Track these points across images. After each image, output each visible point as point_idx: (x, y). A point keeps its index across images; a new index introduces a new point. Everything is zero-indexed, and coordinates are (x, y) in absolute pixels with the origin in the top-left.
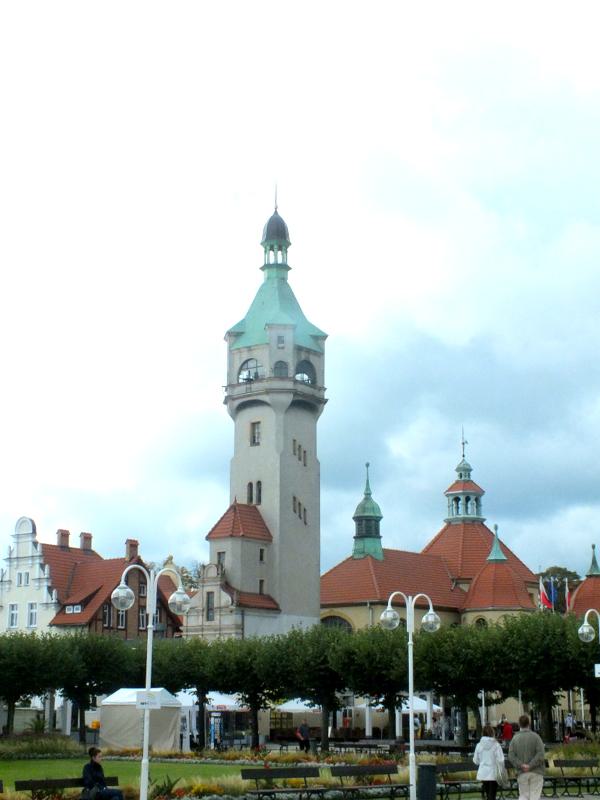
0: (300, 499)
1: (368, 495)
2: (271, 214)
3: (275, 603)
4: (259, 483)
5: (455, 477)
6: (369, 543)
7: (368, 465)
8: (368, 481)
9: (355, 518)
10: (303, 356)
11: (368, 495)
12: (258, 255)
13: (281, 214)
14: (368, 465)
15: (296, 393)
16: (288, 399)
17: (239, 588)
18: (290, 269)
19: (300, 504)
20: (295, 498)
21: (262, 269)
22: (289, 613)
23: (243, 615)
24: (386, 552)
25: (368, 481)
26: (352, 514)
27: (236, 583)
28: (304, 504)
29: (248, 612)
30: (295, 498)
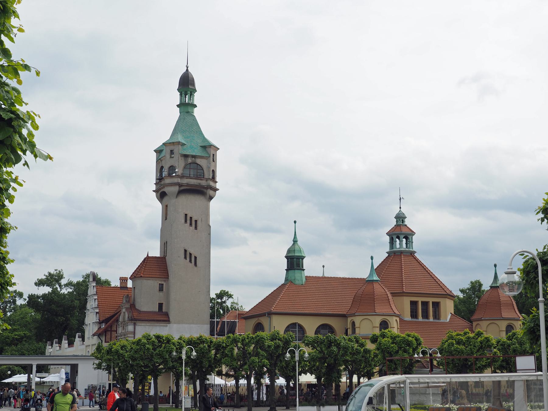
0: (190, 250)
1: (295, 241)
2: (185, 71)
3: (169, 318)
6: (297, 273)
7: (295, 222)
8: (295, 232)
9: (285, 257)
10: (190, 160)
11: (295, 241)
12: (176, 98)
14: (295, 222)
15: (180, 185)
16: (176, 189)
18: (195, 106)
19: (190, 254)
21: (178, 106)
22: (179, 322)
23: (135, 325)
24: (307, 277)
25: (295, 232)
29: (138, 323)
30: (185, 251)
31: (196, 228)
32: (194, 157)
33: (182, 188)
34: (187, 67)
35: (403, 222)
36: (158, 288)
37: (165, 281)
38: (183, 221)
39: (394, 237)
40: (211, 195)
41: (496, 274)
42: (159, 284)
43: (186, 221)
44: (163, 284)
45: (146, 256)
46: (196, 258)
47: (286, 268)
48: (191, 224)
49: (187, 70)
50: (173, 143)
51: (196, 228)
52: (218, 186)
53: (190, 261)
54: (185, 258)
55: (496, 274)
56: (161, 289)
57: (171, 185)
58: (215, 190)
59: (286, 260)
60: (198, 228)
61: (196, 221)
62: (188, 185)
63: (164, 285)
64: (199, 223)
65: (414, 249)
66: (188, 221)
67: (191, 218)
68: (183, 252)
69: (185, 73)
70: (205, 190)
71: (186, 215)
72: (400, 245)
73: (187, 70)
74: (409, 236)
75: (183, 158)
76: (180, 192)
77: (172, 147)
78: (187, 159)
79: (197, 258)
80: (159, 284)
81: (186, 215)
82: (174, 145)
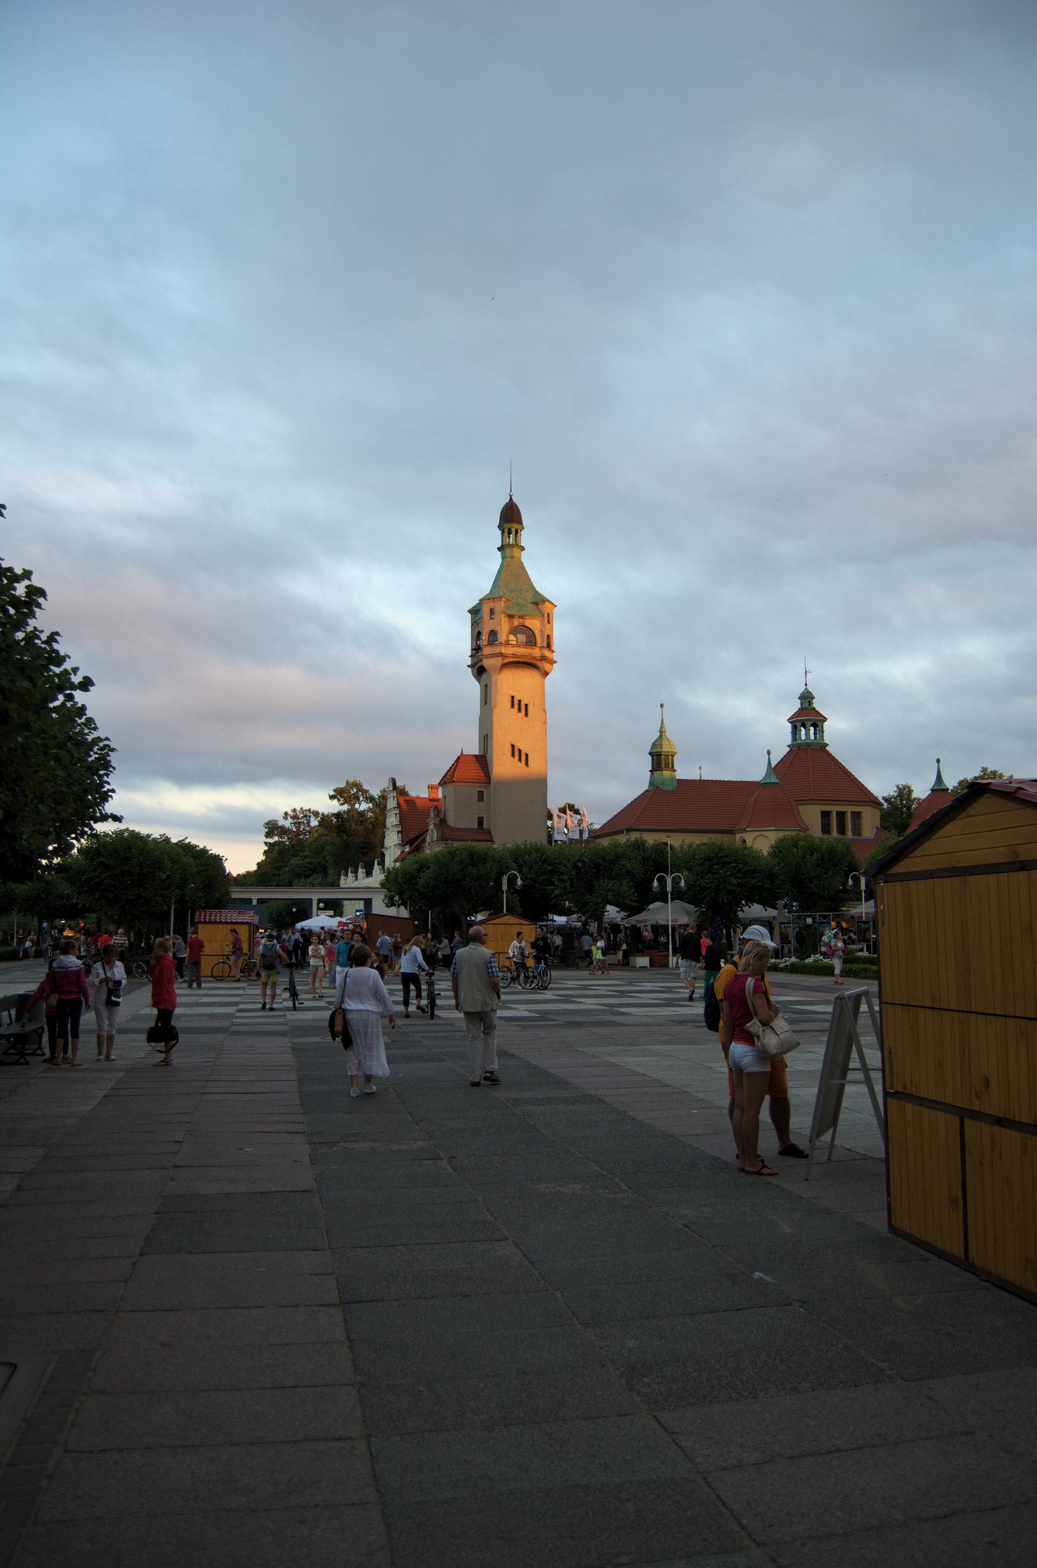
0: (519, 745)
1: (662, 732)
2: (507, 500)
3: (492, 836)
4: (487, 735)
5: (797, 705)
7: (662, 706)
8: (662, 720)
9: (650, 753)
11: (662, 732)
12: (496, 538)
13: (515, 500)
14: (662, 706)
17: (453, 825)
18: (523, 549)
19: (520, 751)
20: (513, 746)
21: (499, 549)
25: (662, 720)
26: (648, 750)
27: (451, 821)
28: (525, 749)
30: (513, 746)
31: (526, 714)
32: (522, 618)
33: (507, 660)
34: (511, 496)
35: (809, 705)
36: (477, 797)
37: (486, 788)
38: (509, 705)
39: (798, 725)
40: (546, 670)
41: (939, 773)
42: (478, 791)
43: (513, 706)
44: (483, 791)
45: (459, 754)
46: (527, 755)
47: (650, 769)
48: (520, 710)
49: (511, 499)
50: (493, 598)
51: (526, 714)
52: (555, 657)
53: (520, 760)
54: (513, 755)
55: (939, 773)
56: (481, 797)
57: (492, 657)
58: (552, 662)
59: (650, 758)
60: (529, 715)
61: (526, 705)
62: (514, 655)
63: (485, 793)
64: (530, 708)
65: (826, 741)
66: (516, 706)
67: (520, 701)
68: (509, 748)
69: (507, 503)
70: (538, 663)
71: (513, 697)
72: (806, 735)
73: (511, 499)
74: (818, 723)
75: (507, 619)
76: (505, 666)
77: (491, 605)
78: (513, 620)
79: (529, 756)
80: (478, 791)
81: (513, 697)
82: (494, 601)
